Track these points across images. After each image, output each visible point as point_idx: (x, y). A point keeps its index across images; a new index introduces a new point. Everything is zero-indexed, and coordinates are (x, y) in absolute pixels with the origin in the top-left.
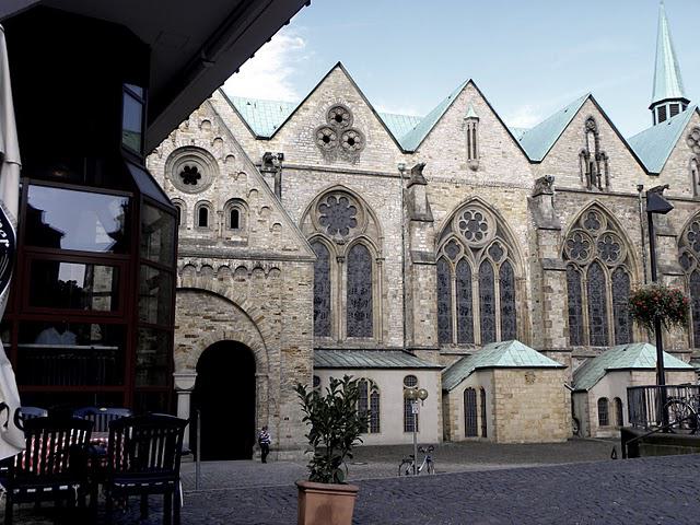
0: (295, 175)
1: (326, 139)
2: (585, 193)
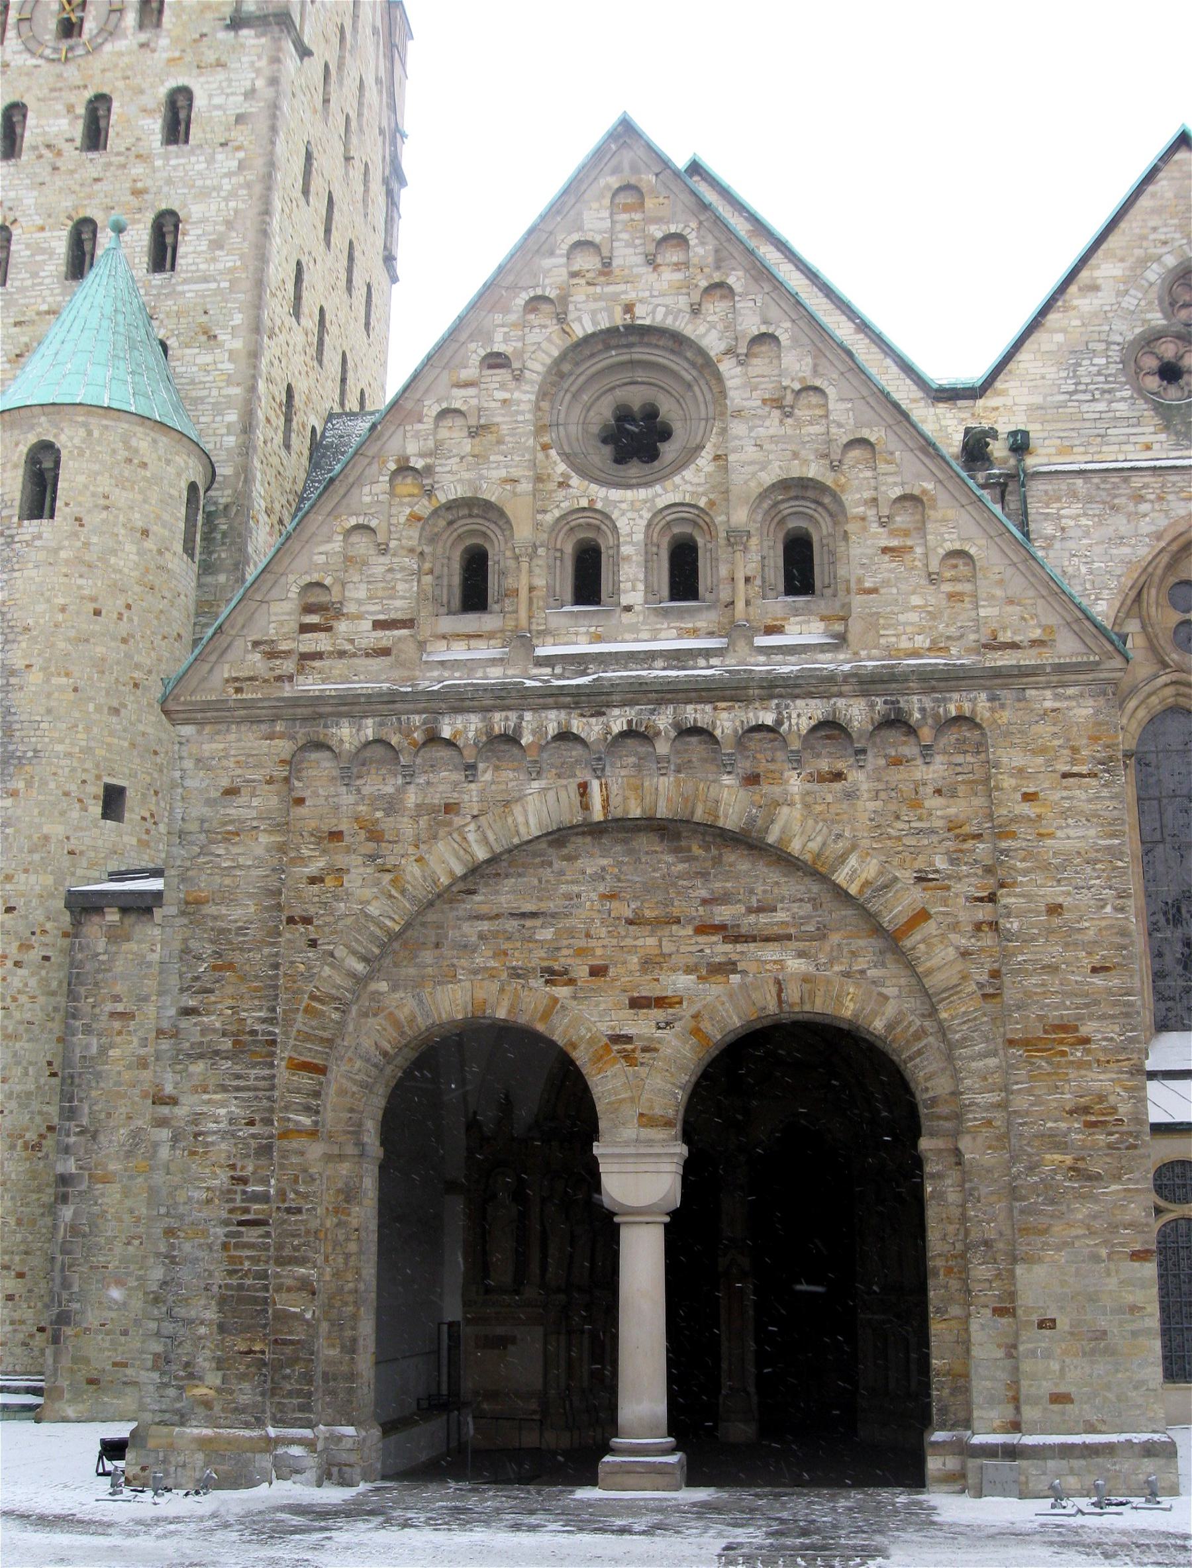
0: (1073, 495)
1: (1170, 372)
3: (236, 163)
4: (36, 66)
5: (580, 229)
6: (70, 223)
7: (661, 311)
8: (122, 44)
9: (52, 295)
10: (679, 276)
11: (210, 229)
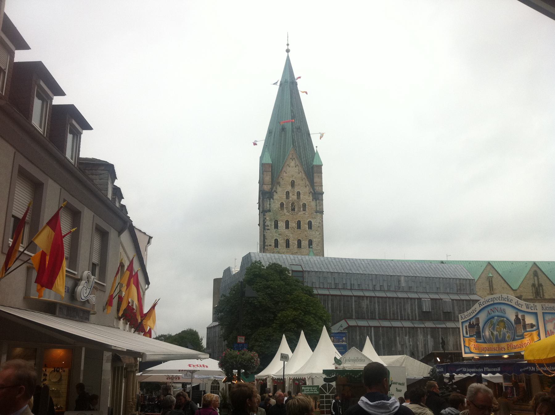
2: (535, 300)
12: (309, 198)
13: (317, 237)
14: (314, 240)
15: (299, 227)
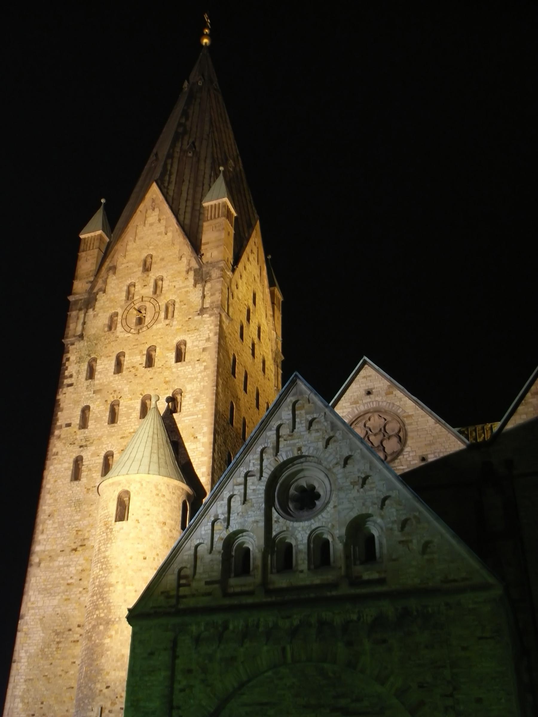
3: (203, 367)
4: (128, 337)
5: (281, 419)
6: (141, 397)
7: (312, 449)
8: (159, 326)
9: (135, 425)
10: (318, 434)
11: (194, 394)
12: (183, 285)
13: (196, 378)
14: (189, 387)
15: (150, 362)
